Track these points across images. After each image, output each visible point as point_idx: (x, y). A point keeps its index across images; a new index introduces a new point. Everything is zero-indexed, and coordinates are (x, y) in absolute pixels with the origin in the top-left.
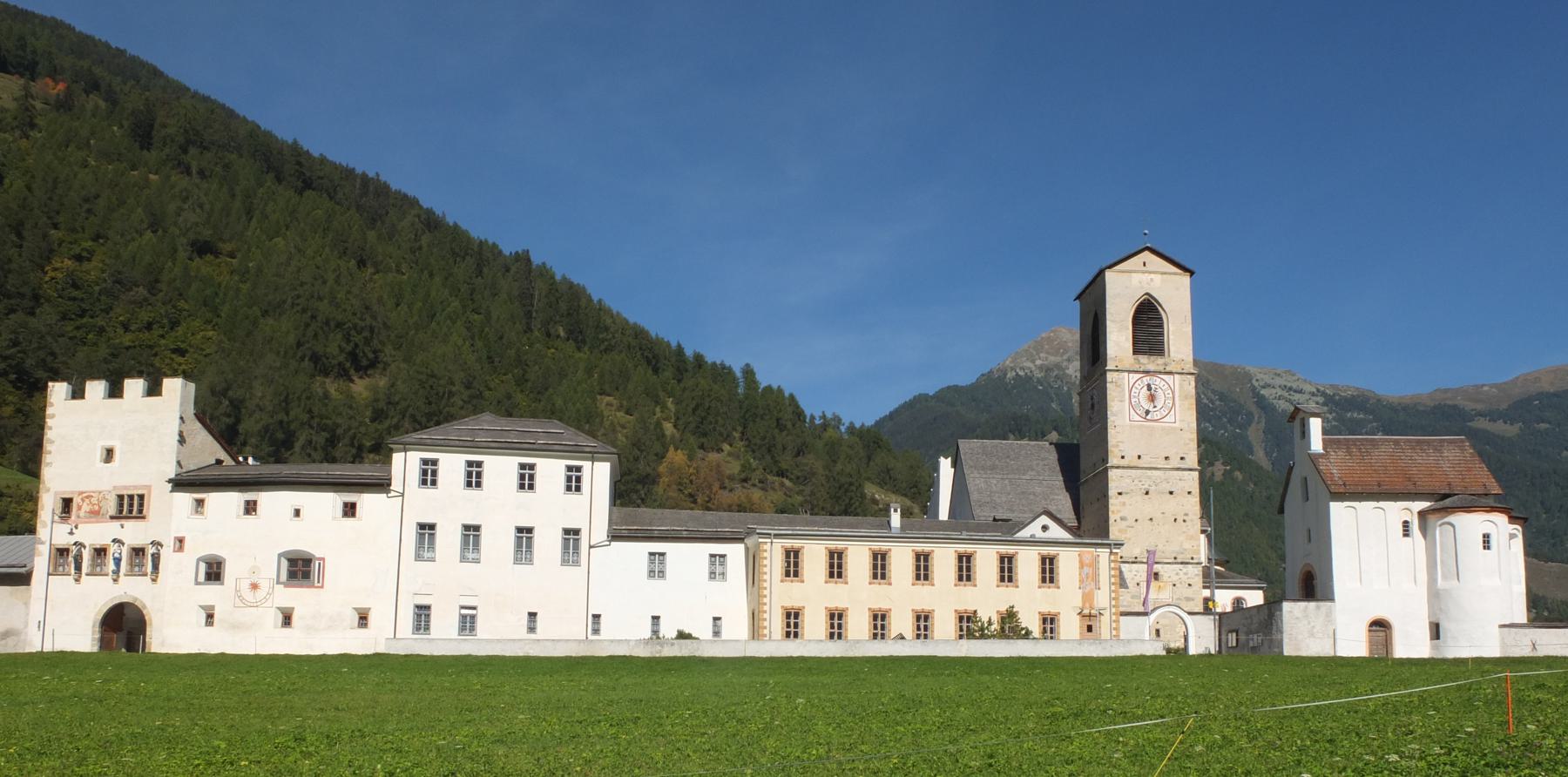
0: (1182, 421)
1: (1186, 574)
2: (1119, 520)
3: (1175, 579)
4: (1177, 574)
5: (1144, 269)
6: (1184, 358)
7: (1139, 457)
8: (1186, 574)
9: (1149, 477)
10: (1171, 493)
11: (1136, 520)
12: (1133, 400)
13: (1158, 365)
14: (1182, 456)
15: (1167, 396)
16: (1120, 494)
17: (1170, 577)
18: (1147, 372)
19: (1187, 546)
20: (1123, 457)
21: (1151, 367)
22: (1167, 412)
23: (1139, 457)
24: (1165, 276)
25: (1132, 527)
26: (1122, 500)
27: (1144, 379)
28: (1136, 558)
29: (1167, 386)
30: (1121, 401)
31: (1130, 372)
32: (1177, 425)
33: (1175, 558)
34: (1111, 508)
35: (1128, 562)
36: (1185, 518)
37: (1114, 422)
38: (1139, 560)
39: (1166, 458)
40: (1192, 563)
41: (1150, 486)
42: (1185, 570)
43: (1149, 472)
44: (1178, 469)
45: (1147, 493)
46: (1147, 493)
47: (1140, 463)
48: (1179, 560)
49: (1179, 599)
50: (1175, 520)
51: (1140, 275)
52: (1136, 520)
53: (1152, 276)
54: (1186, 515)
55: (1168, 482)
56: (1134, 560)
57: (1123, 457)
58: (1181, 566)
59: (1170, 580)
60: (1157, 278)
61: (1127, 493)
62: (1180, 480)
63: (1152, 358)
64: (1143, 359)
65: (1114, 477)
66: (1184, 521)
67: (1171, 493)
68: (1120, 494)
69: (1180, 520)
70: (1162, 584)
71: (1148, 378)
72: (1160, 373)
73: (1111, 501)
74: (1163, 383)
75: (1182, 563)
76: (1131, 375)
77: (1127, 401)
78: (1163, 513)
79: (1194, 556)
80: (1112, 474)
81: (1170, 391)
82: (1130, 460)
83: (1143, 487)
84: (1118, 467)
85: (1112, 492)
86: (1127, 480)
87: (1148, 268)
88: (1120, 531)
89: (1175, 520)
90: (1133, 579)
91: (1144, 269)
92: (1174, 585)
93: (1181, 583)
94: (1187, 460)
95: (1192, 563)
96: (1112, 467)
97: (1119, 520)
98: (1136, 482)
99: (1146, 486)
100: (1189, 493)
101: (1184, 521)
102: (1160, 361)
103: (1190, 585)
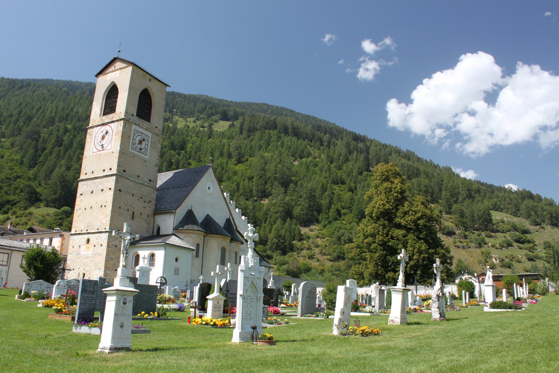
1: (100, 239)
9: (94, 183)
11: (85, 209)
21: (106, 121)
43: (95, 181)
45: (92, 192)
50: (101, 206)
52: (85, 209)
64: (104, 118)
69: (103, 206)
71: (104, 127)
80: (80, 184)
89: (101, 206)
99: (92, 188)
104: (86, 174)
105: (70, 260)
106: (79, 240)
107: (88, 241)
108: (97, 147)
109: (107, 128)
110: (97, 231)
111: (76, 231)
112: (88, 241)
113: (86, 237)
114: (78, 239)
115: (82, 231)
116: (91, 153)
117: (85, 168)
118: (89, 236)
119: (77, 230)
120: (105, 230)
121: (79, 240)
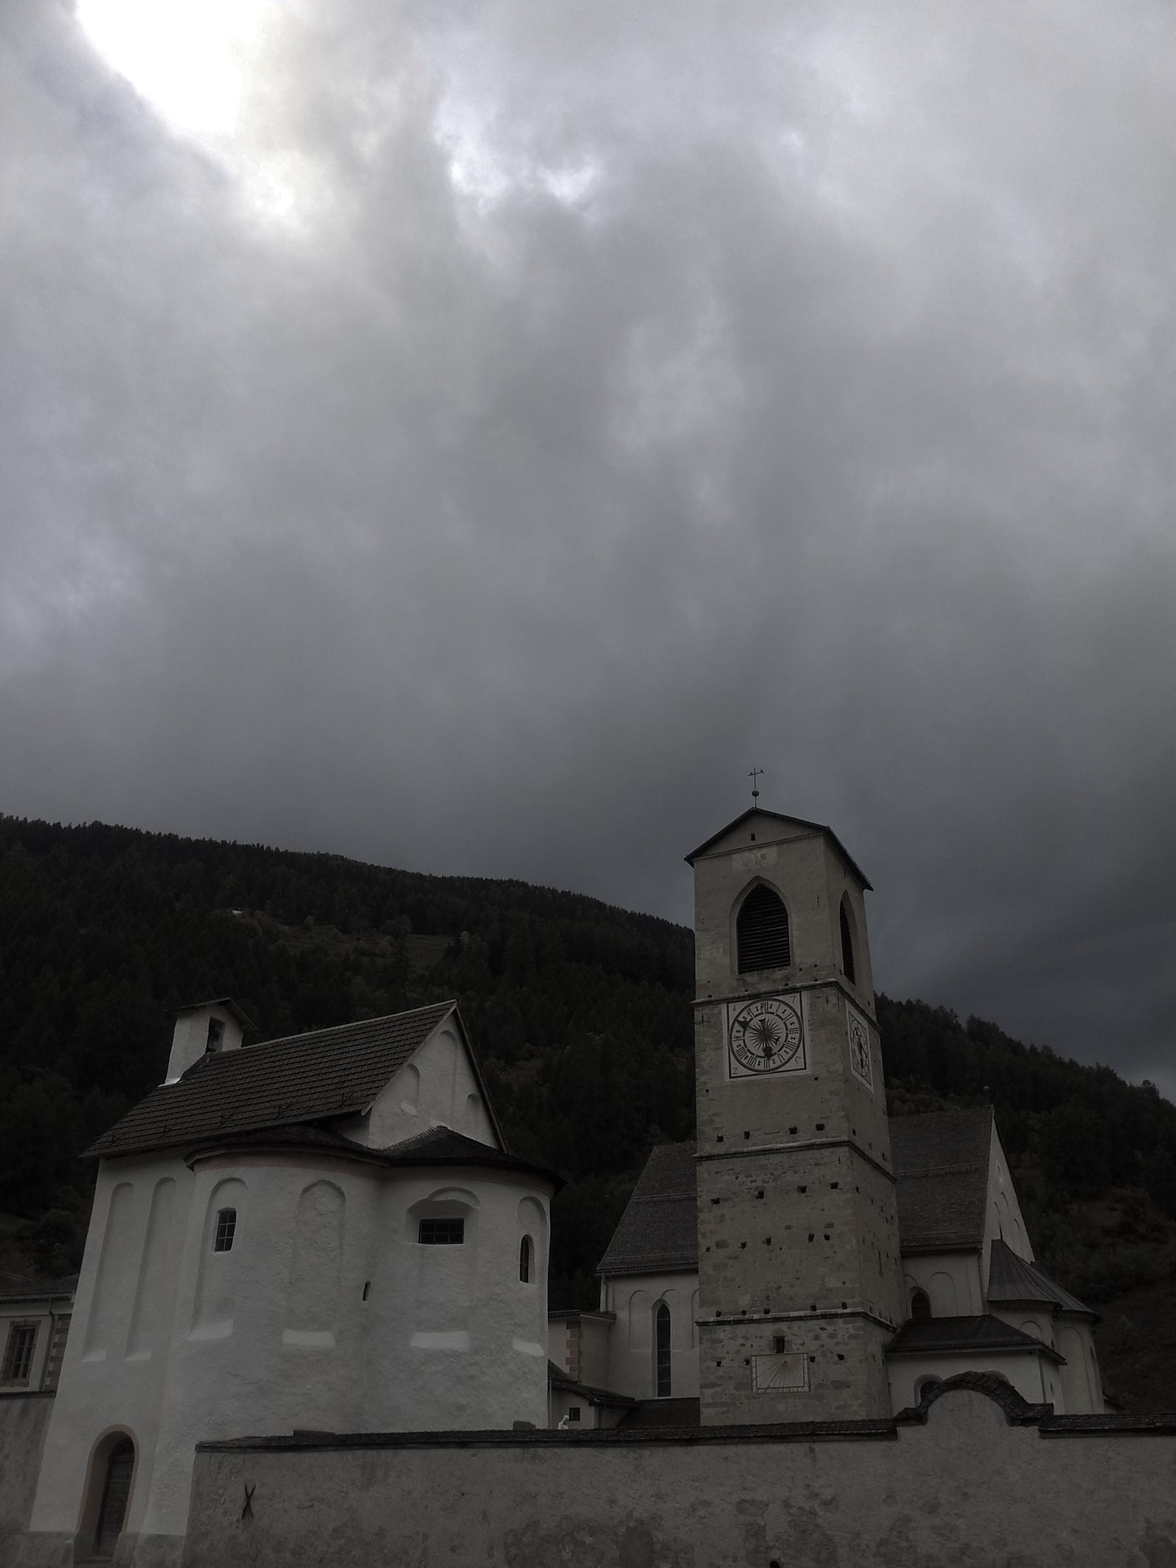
1: (832, 1336)
2: (713, 1249)
4: (817, 1337)
5: (753, 843)
6: (818, 963)
7: (747, 1135)
8: (832, 1336)
10: (803, 1190)
11: (744, 1245)
12: (735, 1044)
13: (774, 981)
14: (821, 1122)
15: (789, 1027)
16: (716, 1202)
17: (803, 1344)
18: (756, 997)
19: (833, 1283)
20: (720, 1139)
21: (764, 987)
22: (791, 1053)
23: (747, 1135)
24: (785, 846)
25: (736, 1258)
27: (753, 1008)
28: (744, 1313)
29: (789, 1011)
30: (717, 1049)
31: (728, 1001)
32: (808, 1072)
33: (814, 1308)
34: (701, 1228)
35: (728, 1323)
36: (829, 1232)
37: (705, 1083)
38: (747, 1316)
39: (793, 1131)
41: (764, 1181)
42: (830, 1329)
43: (763, 1160)
44: (811, 1147)
45: (761, 1195)
46: (761, 1195)
48: (819, 1312)
49: (820, 1386)
50: (811, 1238)
51: (746, 855)
52: (744, 1245)
53: (764, 851)
54: (830, 1225)
55: (796, 1172)
56: (740, 1317)
57: (720, 1139)
58: (823, 1323)
59: (802, 1350)
60: (771, 853)
61: (726, 1200)
62: (816, 1165)
63: (766, 973)
64: (751, 978)
65: (706, 1175)
66: (827, 1238)
67: (803, 1190)
68: (716, 1202)
69: (820, 1236)
70: (789, 1359)
71: (759, 1005)
72: (778, 993)
73: (702, 1216)
74: (783, 1007)
75: (823, 1316)
76: (731, 1006)
77: (726, 1047)
78: (788, 1227)
79: (848, 1301)
81: (794, 1019)
84: (710, 1158)
85: (703, 1200)
86: (727, 1177)
87: (760, 840)
89: (811, 1238)
90: (738, 1352)
91: (753, 843)
92: (812, 1359)
93: (824, 1354)
94: (827, 1128)
95: (842, 1316)
96: (701, 1158)
97: (713, 1249)
98: (742, 1178)
99: (759, 1183)
100: (834, 1186)
101: (827, 1238)
102: (779, 974)
103: (841, 1357)
105: (708, 1405)
106: (742, 1341)
108: (745, 1062)
110: (808, 1313)
111: (719, 1314)
112: (780, 1344)
113: (769, 1330)
114: (733, 1338)
115: (744, 1313)
116: (727, 1079)
118: (783, 1326)
119: (723, 1309)
121: (742, 1341)
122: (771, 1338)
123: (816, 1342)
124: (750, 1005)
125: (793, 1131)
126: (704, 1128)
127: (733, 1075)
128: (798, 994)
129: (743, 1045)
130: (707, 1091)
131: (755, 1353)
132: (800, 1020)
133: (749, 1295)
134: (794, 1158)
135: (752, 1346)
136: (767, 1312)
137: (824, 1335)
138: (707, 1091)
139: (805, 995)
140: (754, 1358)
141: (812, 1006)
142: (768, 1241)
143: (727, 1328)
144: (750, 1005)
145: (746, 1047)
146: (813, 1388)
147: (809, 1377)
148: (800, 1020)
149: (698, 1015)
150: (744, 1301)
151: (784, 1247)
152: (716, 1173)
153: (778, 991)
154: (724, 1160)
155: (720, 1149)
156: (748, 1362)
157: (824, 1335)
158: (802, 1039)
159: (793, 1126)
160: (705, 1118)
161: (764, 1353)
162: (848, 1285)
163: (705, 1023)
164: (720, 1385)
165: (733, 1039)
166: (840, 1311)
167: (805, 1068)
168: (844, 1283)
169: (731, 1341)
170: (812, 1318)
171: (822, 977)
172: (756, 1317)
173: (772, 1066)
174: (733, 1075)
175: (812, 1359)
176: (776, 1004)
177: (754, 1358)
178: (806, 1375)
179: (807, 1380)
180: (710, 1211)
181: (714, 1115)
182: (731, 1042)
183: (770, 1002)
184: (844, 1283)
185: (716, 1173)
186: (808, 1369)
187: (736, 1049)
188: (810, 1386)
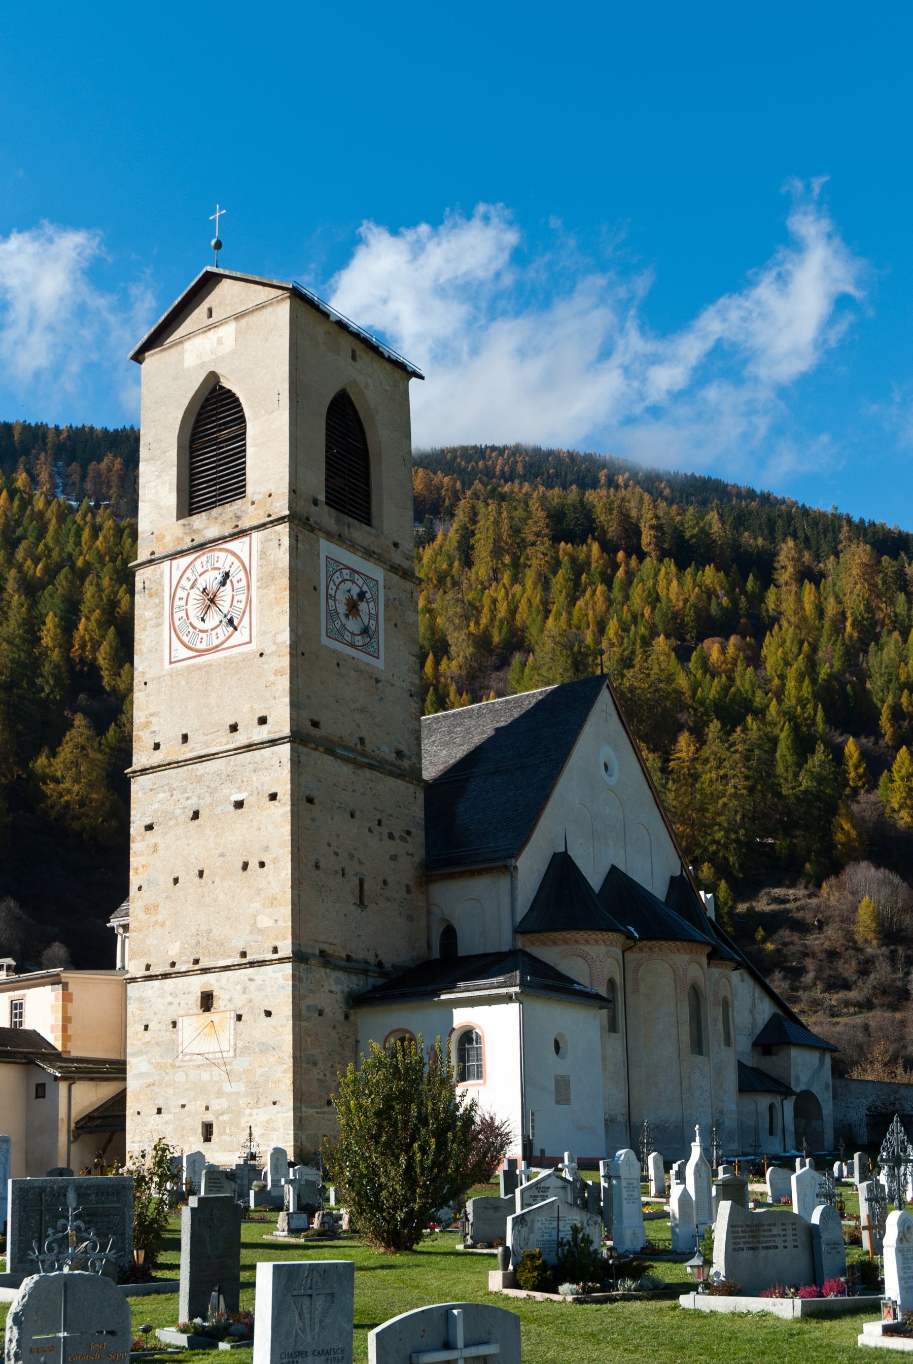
0: (263, 633)
3: (240, 1003)
7: (185, 738)
8: (260, 988)
9: (200, 779)
10: (239, 805)
11: (176, 881)
12: (177, 616)
23: (185, 738)
26: (154, 841)
27: (198, 564)
28: (173, 964)
33: (244, 954)
40: (271, 962)
44: (249, 747)
45: (196, 815)
47: (187, 752)
48: (249, 958)
50: (245, 866)
72: (224, 539)
75: (252, 964)
79: (279, 944)
82: (172, 751)
83: (189, 802)
88: (147, 910)
92: (239, 1018)
98: (177, 795)
99: (194, 800)
104: (157, 746)
106: (170, 999)
107: (207, 1001)
109: (222, 559)
110: (238, 960)
111: (148, 967)
112: (207, 1001)
113: (197, 984)
114: (162, 996)
117: (148, 723)
120: (276, 956)
122: (200, 994)
123: (244, 996)
124: (195, 559)
125: (234, 728)
126: (140, 733)
127: (173, 660)
128: (247, 539)
129: (185, 617)
130: (146, 683)
131: (182, 1012)
132: (248, 574)
133: (178, 944)
134: (232, 763)
135: (179, 1004)
136: (196, 962)
137: (252, 986)
138: (146, 683)
139: (255, 535)
140: (180, 1019)
141: (263, 554)
142: (201, 874)
143: (156, 983)
144: (195, 559)
145: (188, 619)
146: (238, 1052)
147: (235, 1039)
148: (248, 574)
149: (140, 577)
150: (173, 951)
151: (217, 880)
152: (151, 790)
153: (225, 537)
154: (159, 773)
155: (158, 758)
156: (174, 1024)
157: (252, 986)
158: (249, 601)
159: (233, 722)
160: (142, 720)
161: (191, 1012)
162: (279, 923)
163: (147, 592)
164: (147, 1052)
165: (175, 610)
166: (271, 956)
167: (250, 642)
168: (276, 921)
169: (159, 1000)
170: (240, 966)
171: (276, 510)
172: (183, 969)
173: (216, 642)
174: (173, 660)
175: (239, 1018)
176: (222, 555)
177: (180, 1019)
178: (232, 1037)
179: (232, 1043)
180: (143, 840)
181: (152, 715)
182: (172, 614)
183: (217, 554)
184: (276, 921)
185: (151, 790)
186: (235, 1029)
187: (177, 623)
188: (235, 1051)
